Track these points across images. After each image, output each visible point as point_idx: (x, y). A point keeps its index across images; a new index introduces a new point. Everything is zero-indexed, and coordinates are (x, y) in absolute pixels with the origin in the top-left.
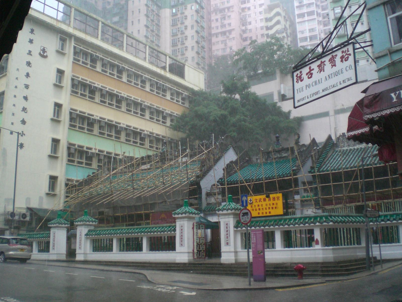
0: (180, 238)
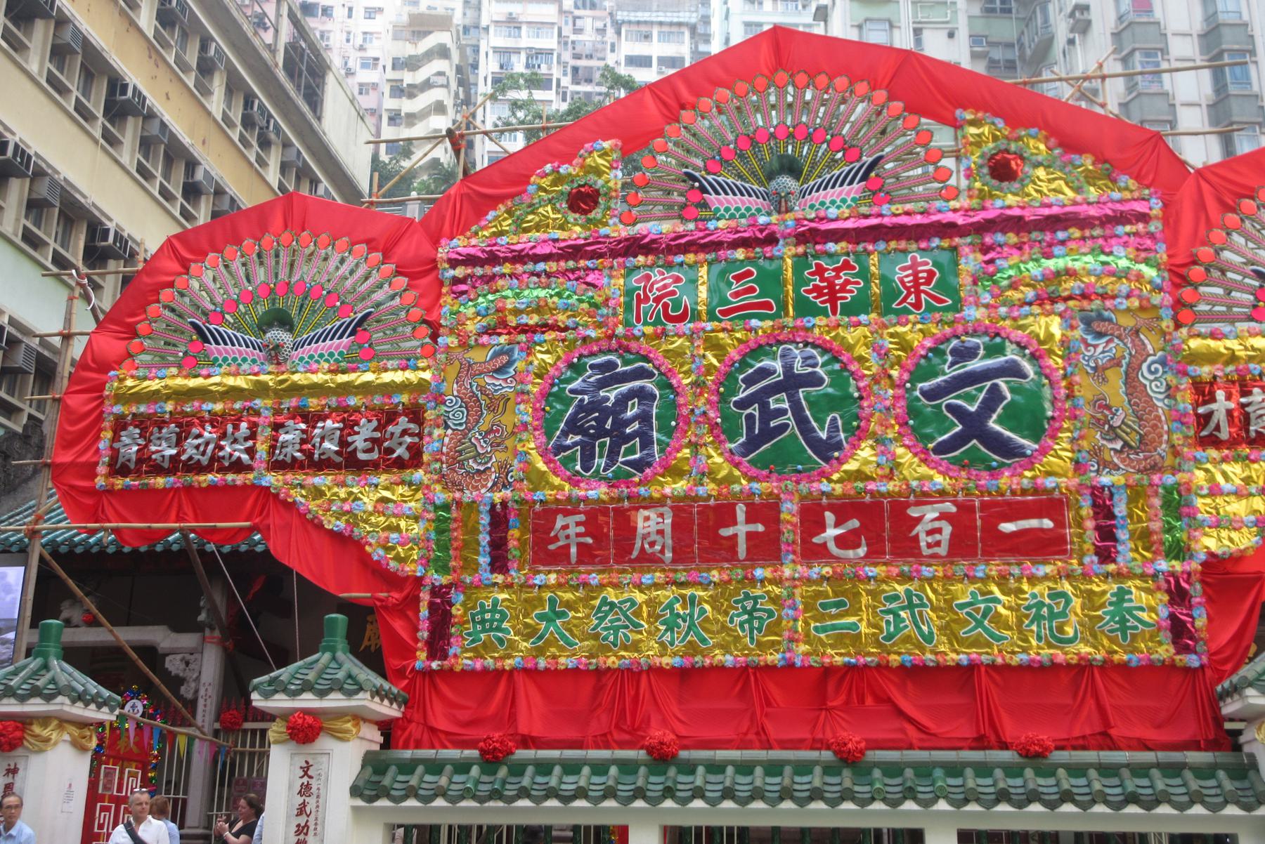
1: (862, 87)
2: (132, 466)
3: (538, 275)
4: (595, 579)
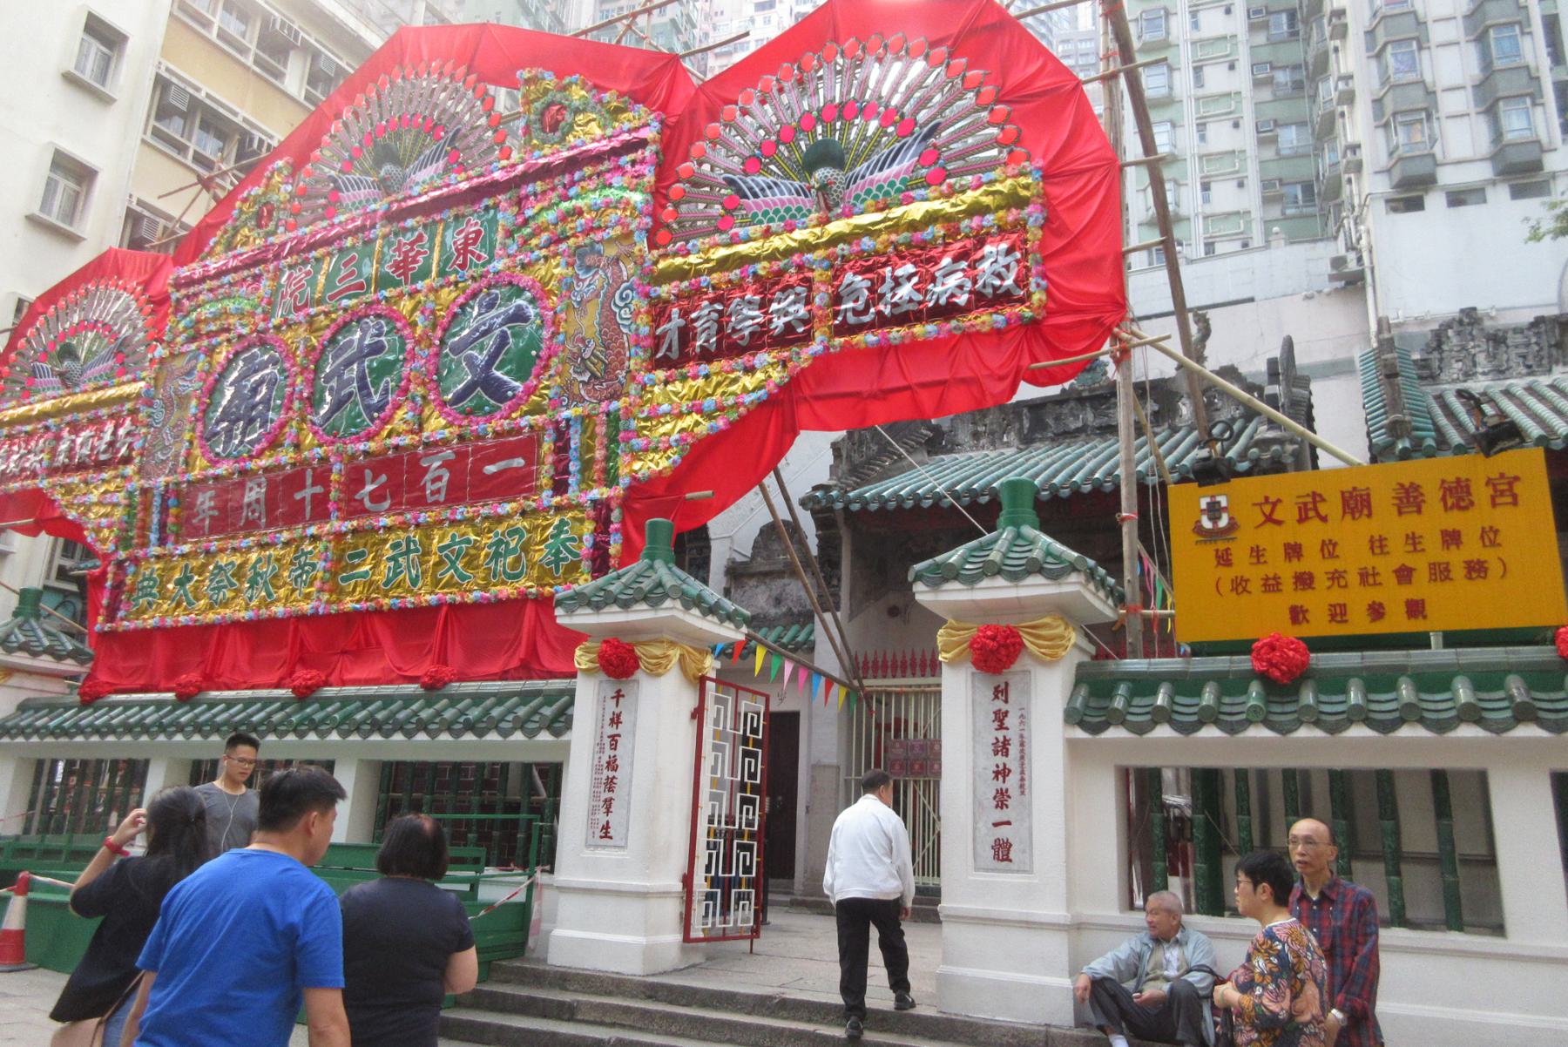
0: (596, 783)
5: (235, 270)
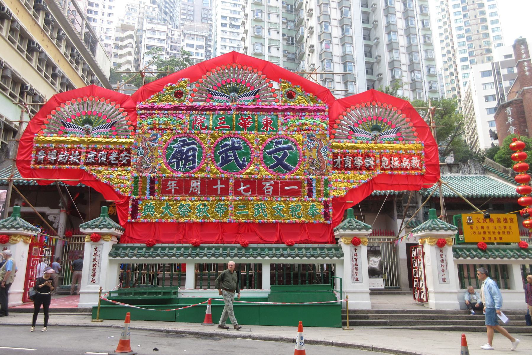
0: (352, 269)
1: (255, 70)
2: (42, 162)
3: (165, 114)
4: (179, 198)
5: (168, 110)
